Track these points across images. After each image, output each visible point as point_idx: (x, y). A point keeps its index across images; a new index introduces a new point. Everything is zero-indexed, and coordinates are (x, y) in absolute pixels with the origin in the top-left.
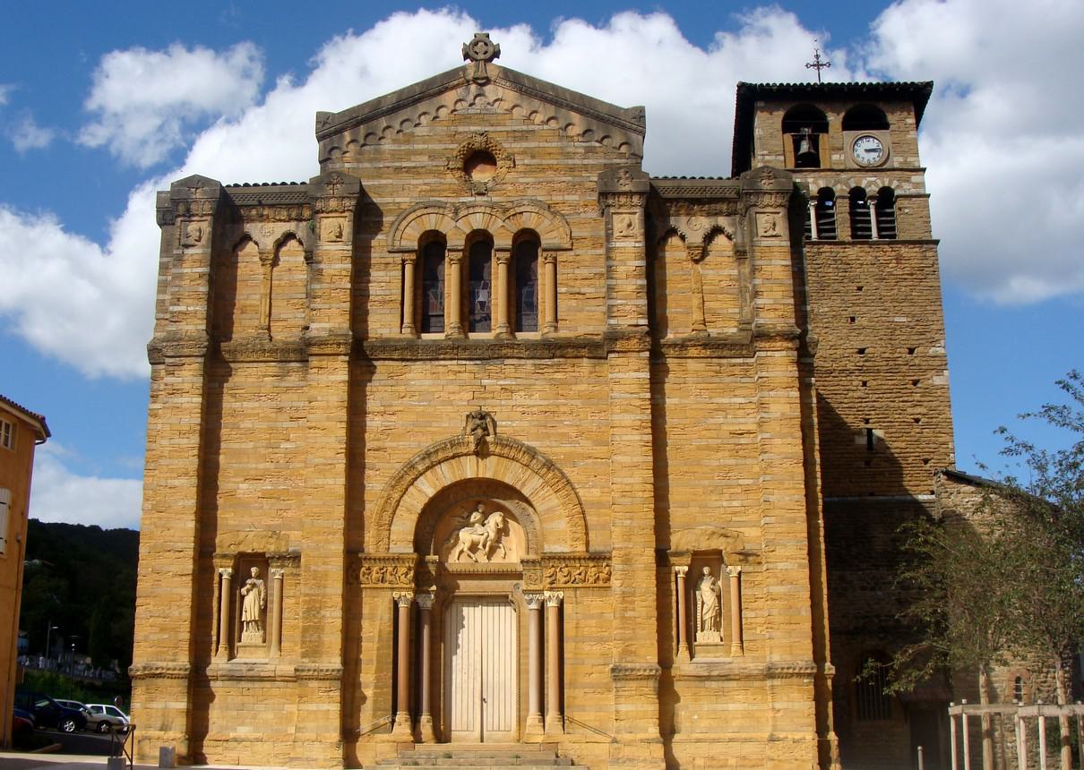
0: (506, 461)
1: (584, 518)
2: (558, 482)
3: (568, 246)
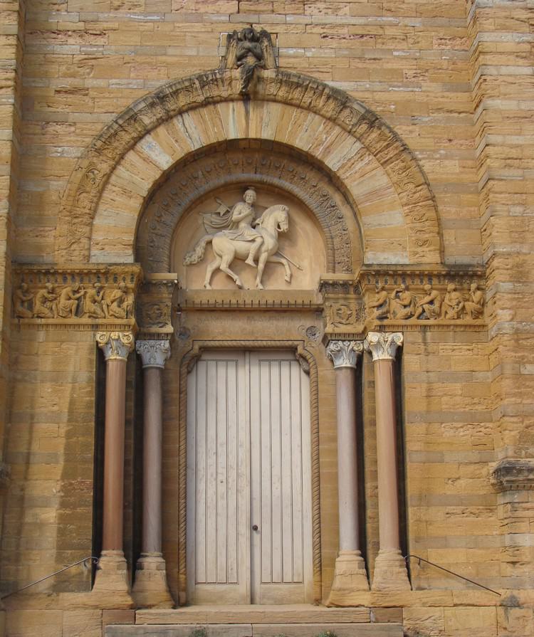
0: (295, 112)
1: (435, 207)
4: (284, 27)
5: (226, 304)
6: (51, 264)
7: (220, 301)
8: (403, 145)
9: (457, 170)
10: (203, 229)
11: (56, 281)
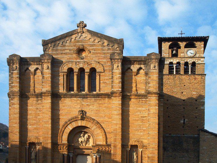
3: (103, 71)
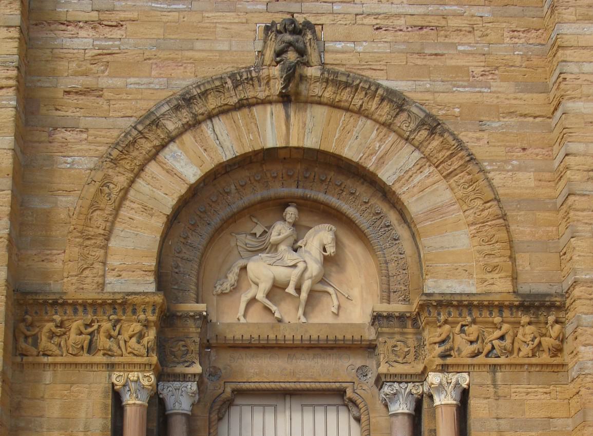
0: (343, 116)
1: (507, 227)
2: (451, 156)
4: (331, 17)
5: (263, 340)
6: (59, 293)
7: (256, 337)
8: (469, 155)
9: (533, 184)
10: (236, 252)
11: (65, 313)
